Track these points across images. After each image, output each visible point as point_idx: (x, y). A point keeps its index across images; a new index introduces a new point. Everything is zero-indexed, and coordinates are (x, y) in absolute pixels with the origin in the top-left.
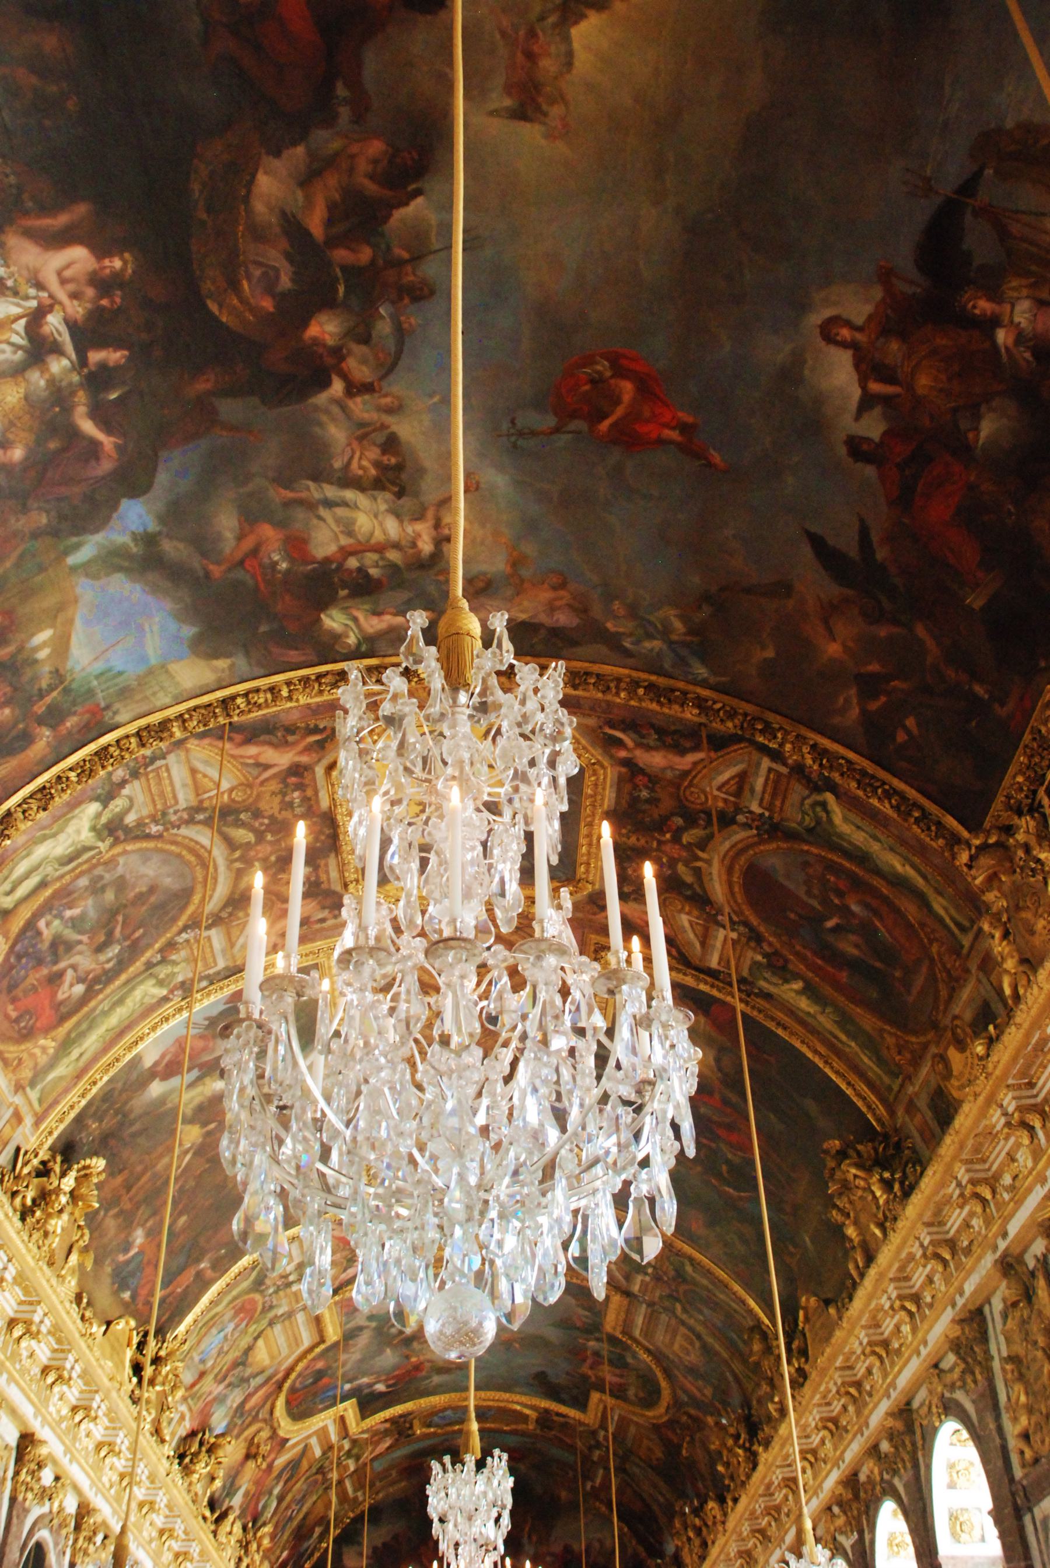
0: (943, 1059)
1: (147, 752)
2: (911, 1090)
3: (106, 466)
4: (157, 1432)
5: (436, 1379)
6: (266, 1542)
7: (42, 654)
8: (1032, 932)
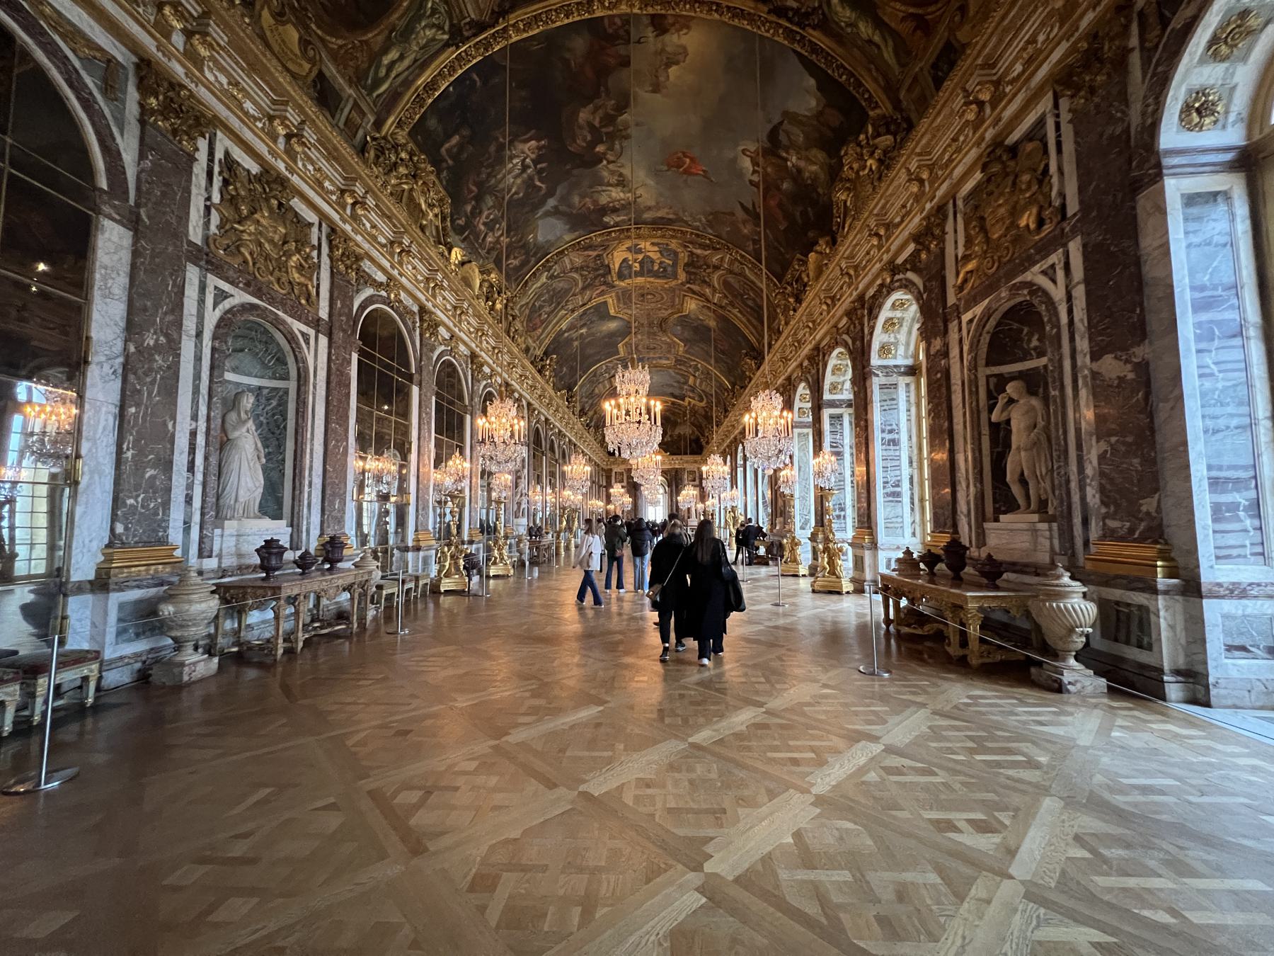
3: (543, 192)
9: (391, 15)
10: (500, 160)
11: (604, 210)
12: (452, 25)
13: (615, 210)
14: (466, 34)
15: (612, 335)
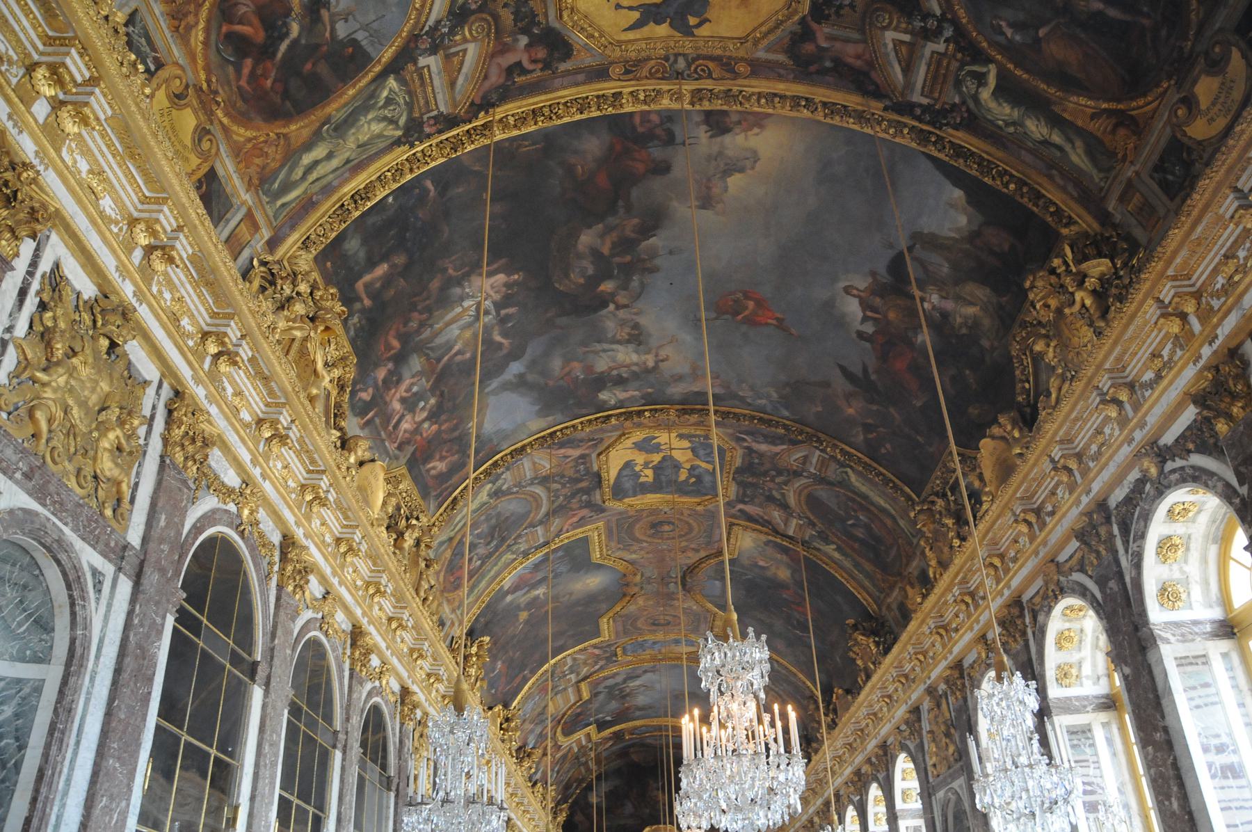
5: (638, 713)
9: (329, 104)
10: (444, 301)
11: (601, 382)
12: (411, 120)
13: (620, 382)
14: (427, 130)
15: (591, 599)
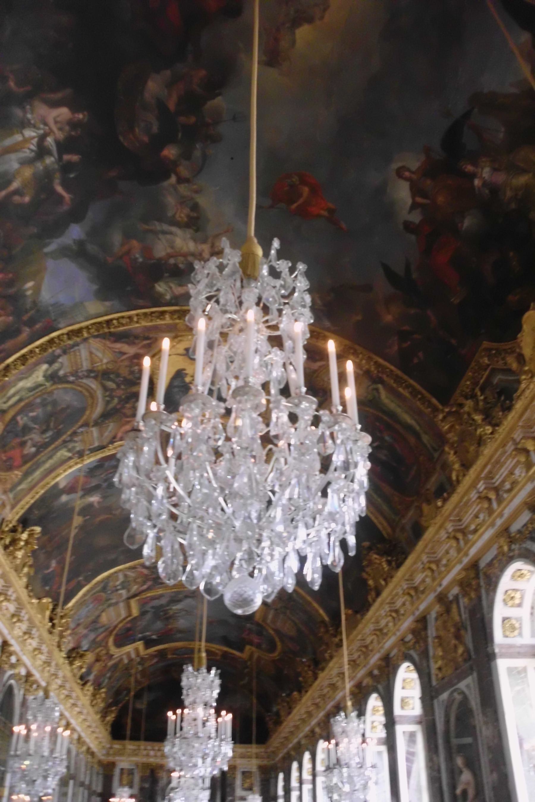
0: (420, 508)
1: (70, 342)
2: (404, 521)
3: (65, 208)
4: (59, 646)
5: (179, 635)
6: (103, 695)
7: (29, 293)
8: (468, 452)
